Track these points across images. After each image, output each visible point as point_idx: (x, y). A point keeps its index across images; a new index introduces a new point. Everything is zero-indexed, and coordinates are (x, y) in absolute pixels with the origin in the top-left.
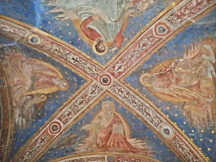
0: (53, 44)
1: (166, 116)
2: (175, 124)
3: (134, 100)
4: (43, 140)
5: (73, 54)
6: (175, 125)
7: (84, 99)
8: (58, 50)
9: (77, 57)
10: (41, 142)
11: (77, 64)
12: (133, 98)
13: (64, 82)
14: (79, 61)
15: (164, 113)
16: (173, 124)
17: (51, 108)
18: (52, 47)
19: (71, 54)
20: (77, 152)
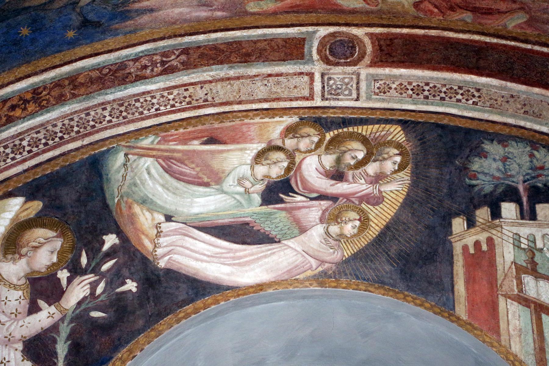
20: (145, 18)
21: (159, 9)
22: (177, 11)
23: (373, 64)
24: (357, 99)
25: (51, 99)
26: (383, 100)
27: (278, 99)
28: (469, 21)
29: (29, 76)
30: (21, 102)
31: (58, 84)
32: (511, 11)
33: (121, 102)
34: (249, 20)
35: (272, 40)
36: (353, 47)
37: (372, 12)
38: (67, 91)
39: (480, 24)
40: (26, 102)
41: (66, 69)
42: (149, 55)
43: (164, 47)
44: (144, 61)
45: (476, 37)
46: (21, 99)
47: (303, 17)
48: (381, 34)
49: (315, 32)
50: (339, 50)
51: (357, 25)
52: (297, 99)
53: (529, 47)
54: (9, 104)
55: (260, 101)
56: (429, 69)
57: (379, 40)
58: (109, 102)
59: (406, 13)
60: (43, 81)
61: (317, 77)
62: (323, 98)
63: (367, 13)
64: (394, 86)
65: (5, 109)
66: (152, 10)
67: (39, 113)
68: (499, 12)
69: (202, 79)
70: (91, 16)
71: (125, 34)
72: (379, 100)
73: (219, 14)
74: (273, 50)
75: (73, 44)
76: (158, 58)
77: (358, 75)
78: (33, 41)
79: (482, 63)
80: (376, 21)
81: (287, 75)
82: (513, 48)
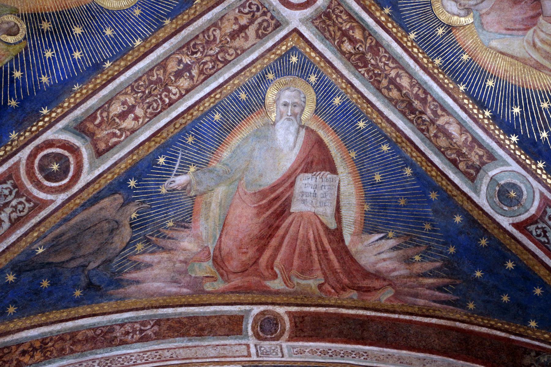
1: (510, 140)
2: (541, 165)
3: (398, 75)
6: (540, 169)
7: (199, 55)
12: (394, 68)
15: (501, 127)
16: (534, 167)
17: (44, 79)
20: (132, 289)
21: (143, 282)
22: (156, 284)
23: (291, 339)
24: (283, 357)
25: (54, 351)
26: (301, 357)
27: (226, 357)
28: (355, 298)
29: (40, 325)
30: (31, 349)
31: (61, 337)
32: (382, 288)
33: (107, 359)
34: (205, 298)
35: (220, 317)
36: (277, 324)
37: (290, 293)
38: (67, 345)
39: (363, 300)
40: (35, 349)
41: (70, 324)
42: (132, 321)
43: (143, 317)
44: (128, 328)
45: (361, 312)
46: (31, 346)
47: (242, 297)
48: (296, 312)
49: (250, 311)
50: (267, 327)
51: (279, 304)
52: (239, 357)
53: (396, 316)
54: (21, 349)
55: (212, 358)
56: (329, 342)
57: (294, 317)
58: (98, 359)
59: (313, 293)
60: (51, 332)
61: (252, 346)
62: (258, 356)
63: (287, 294)
64: (307, 351)
65: (17, 353)
66: (138, 282)
67: (43, 363)
68: (376, 289)
69: (168, 347)
70: (95, 280)
71: (117, 300)
72: (298, 357)
73: (185, 290)
74: (221, 326)
75: (78, 302)
76: (137, 326)
77: (281, 346)
78: (50, 293)
79: (366, 334)
80: (292, 300)
81: (230, 345)
82: (386, 319)
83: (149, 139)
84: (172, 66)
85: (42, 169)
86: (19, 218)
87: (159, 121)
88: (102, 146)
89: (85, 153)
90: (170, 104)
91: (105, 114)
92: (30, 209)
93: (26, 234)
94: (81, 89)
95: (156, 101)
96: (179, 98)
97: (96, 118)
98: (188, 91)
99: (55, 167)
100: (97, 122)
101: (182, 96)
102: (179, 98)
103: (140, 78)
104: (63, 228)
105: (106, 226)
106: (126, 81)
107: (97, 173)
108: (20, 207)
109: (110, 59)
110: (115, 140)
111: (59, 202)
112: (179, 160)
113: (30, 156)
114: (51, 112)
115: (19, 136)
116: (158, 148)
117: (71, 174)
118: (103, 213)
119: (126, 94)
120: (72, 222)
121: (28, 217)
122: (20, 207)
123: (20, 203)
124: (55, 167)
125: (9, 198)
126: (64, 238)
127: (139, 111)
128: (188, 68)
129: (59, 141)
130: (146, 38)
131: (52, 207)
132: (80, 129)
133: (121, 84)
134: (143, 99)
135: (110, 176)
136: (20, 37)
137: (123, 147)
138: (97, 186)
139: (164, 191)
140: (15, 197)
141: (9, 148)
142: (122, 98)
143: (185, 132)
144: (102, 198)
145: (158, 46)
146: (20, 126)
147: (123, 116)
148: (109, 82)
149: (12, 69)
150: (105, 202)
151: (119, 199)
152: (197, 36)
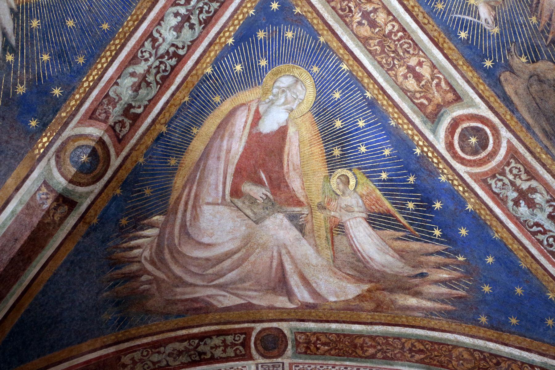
0: (111, 94)
4: (524, 196)
5: (158, 27)
8: (136, 80)
9: (169, 14)
10: (531, 204)
11: (203, 16)
13: (277, 84)
14: (189, 7)
17: (387, 152)
18: (120, 99)
19: (156, 35)
83: (441, 50)
84: (365, 31)
85: (475, 152)
86: (526, 172)
87: (421, 41)
88: (450, 96)
89: (458, 112)
90: (404, 30)
91: (418, 95)
92: (517, 161)
93: (544, 165)
94: (394, 118)
95: (401, 45)
96: (397, 21)
97: (422, 104)
98: (389, 13)
99: (473, 140)
100: (426, 102)
101: (395, 19)
102: (397, 21)
103: (379, 63)
104: (537, 130)
105: (535, 87)
106: (383, 77)
107: (478, 100)
108: (515, 171)
109: (363, 92)
110: (443, 84)
111: (509, 135)
112: (462, 16)
113: (463, 164)
114: (418, 145)
115: (443, 173)
116: (450, 39)
117: (480, 125)
118: (521, 91)
119: (396, 75)
120: (530, 121)
121: (526, 164)
122: (515, 171)
123: (511, 171)
124: (473, 140)
125: (507, 181)
126: (548, 128)
127: (413, 62)
128: (366, 15)
129: (446, 137)
130: (340, 59)
131: (515, 141)
132: (434, 118)
133: (386, 81)
134: (400, 58)
135: (482, 87)
136: (350, 174)
137: (451, 75)
138: (492, 99)
139: (496, 30)
140: (505, 176)
141: (456, 183)
142: (400, 79)
143: (432, 13)
144: (505, 93)
145: (346, 47)
146: (433, 173)
147: (418, 77)
148: (385, 93)
149: (380, 181)
150: (509, 90)
151: (505, 76)
152: (333, 8)
